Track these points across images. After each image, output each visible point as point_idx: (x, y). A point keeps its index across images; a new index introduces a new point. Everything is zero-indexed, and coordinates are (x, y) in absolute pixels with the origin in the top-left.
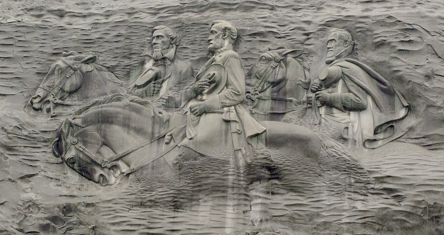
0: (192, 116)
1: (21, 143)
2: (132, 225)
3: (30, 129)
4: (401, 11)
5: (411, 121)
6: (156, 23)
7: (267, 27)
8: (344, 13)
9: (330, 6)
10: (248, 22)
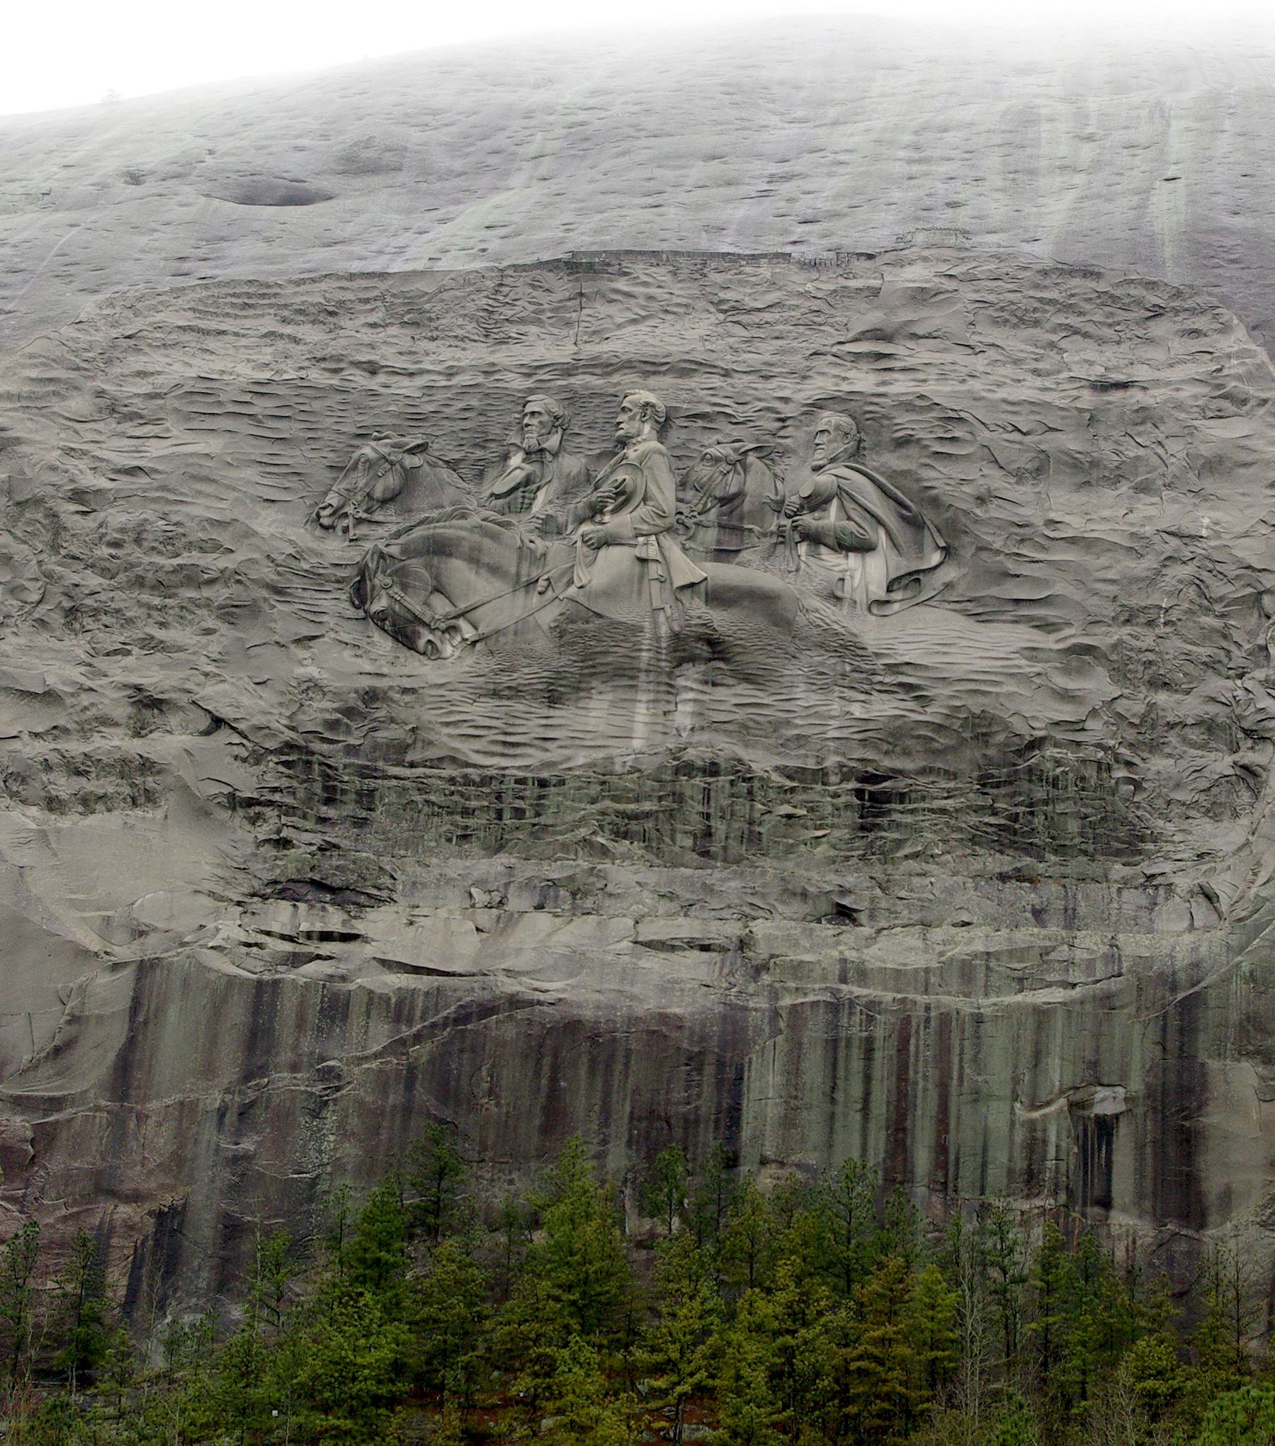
0: (585, 549)
1: (297, 583)
2: (476, 727)
3: (314, 560)
4: (940, 388)
5: (950, 573)
6: (531, 391)
7: (715, 404)
8: (845, 387)
9: (823, 374)
10: (684, 395)
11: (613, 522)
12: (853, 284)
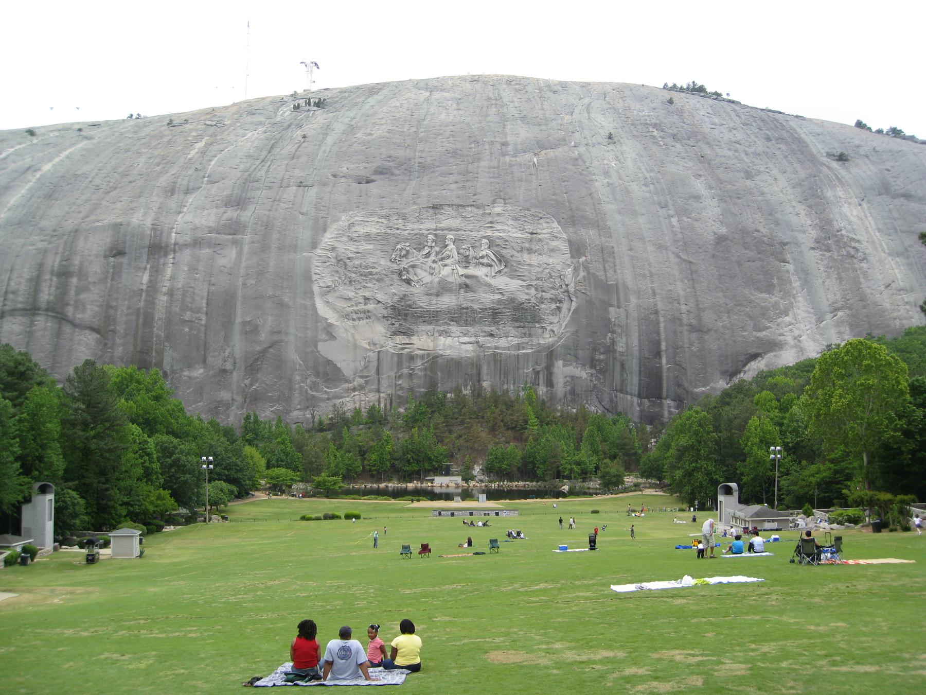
5: (506, 270)
11: (447, 262)
12: (487, 212)
